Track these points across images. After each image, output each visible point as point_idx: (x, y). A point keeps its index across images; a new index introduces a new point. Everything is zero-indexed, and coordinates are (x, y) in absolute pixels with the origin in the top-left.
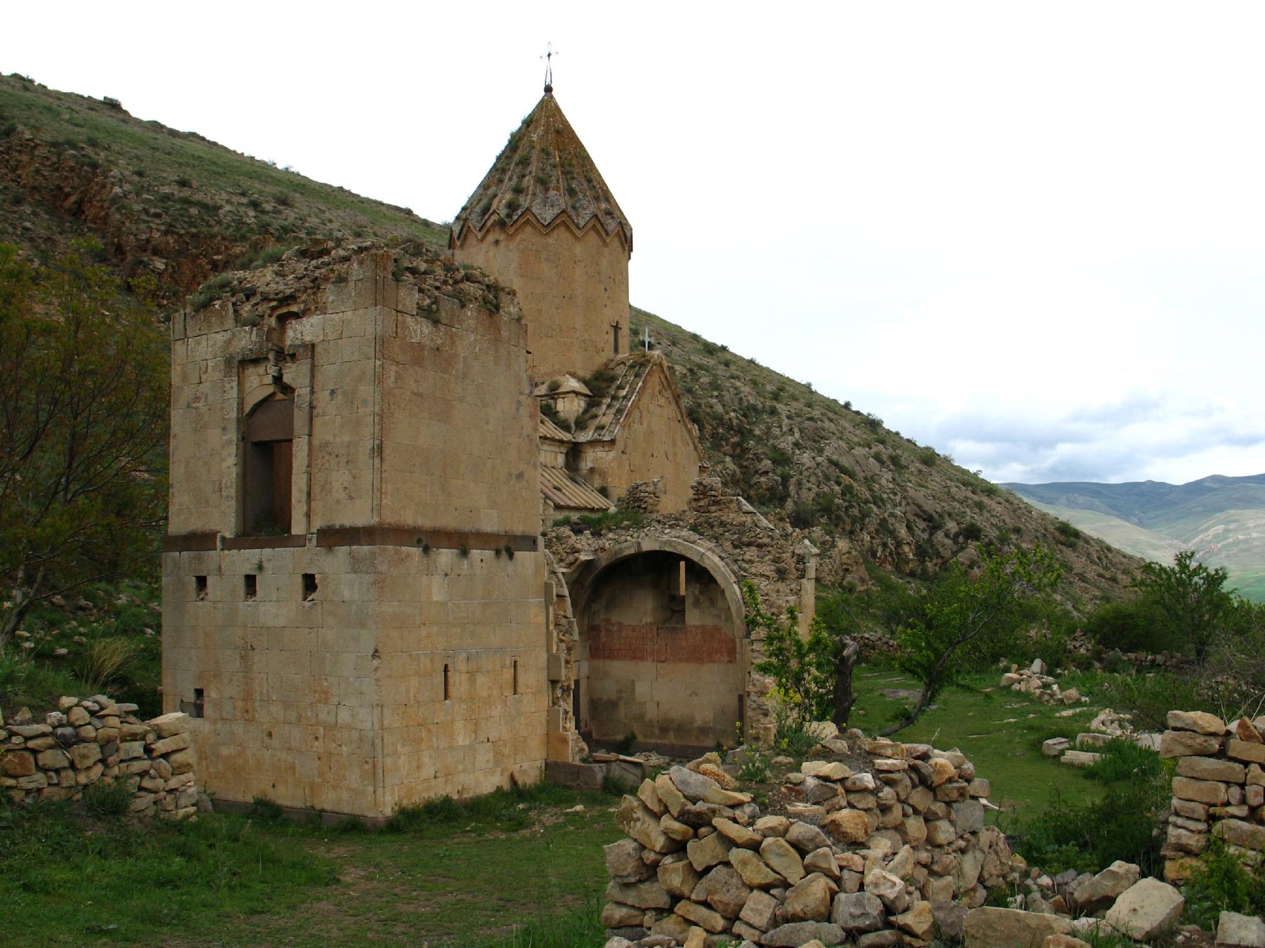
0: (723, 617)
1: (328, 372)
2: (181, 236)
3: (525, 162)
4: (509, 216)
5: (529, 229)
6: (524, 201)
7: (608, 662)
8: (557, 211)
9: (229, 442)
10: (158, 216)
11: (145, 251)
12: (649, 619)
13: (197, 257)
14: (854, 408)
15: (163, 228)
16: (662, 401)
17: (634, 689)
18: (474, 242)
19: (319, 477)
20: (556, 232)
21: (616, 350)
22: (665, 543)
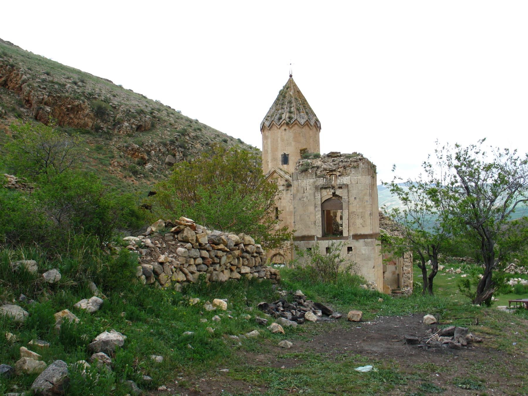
1: (354, 192)
2: (54, 97)
3: (290, 102)
4: (290, 121)
5: (296, 126)
6: (295, 117)
8: (305, 120)
9: (318, 210)
10: (44, 89)
11: (41, 103)
13: (61, 106)
15: (47, 94)
18: (276, 128)
19: (352, 221)
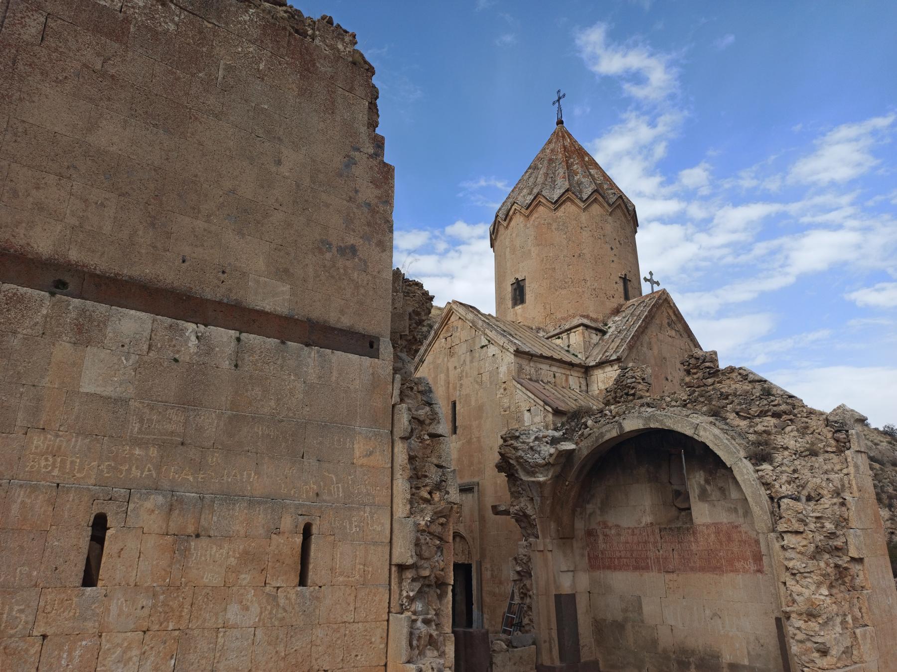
0: (741, 511)
7: (608, 573)
8: (562, 191)
12: (648, 519)
14: (873, 426)
16: (673, 333)
17: (640, 607)
20: (563, 207)
21: (627, 298)
22: (649, 418)
